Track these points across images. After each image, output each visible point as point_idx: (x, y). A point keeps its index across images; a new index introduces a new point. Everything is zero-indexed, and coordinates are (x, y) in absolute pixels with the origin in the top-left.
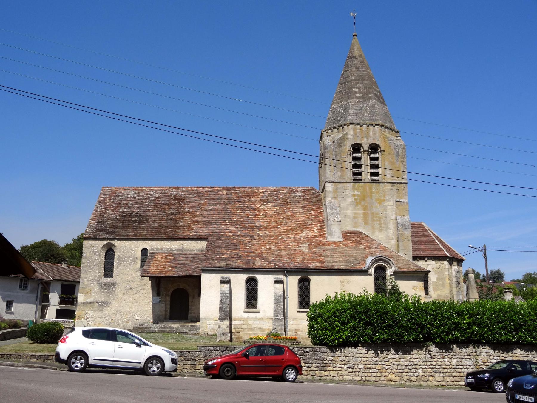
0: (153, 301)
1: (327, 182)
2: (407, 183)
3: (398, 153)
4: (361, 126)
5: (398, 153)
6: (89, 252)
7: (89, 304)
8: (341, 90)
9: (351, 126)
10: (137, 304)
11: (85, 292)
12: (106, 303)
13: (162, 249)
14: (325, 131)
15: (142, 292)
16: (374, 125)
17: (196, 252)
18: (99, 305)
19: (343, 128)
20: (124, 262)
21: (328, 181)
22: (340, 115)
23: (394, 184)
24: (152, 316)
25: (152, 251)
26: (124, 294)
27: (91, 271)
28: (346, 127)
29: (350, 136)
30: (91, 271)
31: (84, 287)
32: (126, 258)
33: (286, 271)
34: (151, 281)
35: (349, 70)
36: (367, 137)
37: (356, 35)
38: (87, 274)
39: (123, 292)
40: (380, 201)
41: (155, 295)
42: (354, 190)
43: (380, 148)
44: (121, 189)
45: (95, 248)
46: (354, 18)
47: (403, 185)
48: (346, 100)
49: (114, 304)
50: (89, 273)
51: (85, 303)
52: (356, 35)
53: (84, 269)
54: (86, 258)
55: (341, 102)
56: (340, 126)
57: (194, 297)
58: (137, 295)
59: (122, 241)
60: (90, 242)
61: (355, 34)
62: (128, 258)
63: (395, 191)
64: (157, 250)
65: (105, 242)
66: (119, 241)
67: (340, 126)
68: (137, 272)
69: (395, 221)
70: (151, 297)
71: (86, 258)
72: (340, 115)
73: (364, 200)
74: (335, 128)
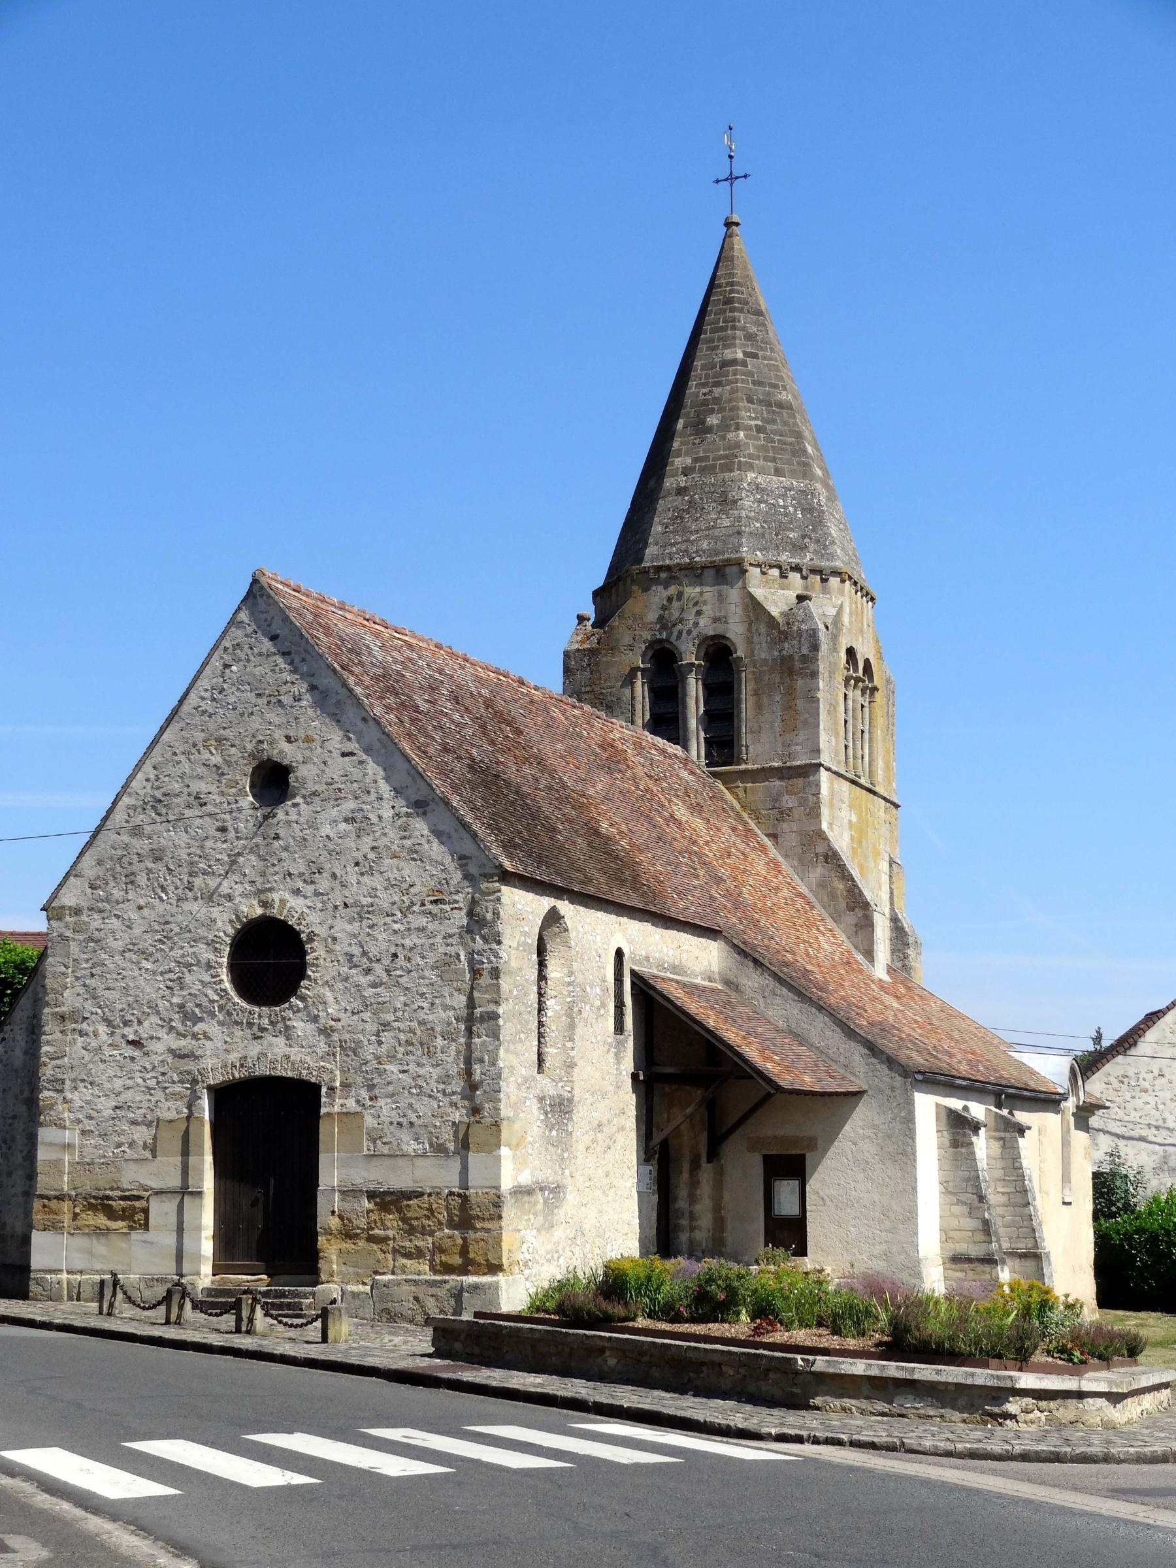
0: (639, 1181)
1: (822, 765)
2: (897, 806)
3: (888, 707)
4: (856, 592)
5: (888, 707)
6: (515, 945)
7: (526, 1198)
8: (760, 423)
9: (848, 582)
10: (611, 1193)
11: (514, 1142)
12: (557, 1190)
13: (647, 958)
14: (759, 565)
15: (620, 1138)
16: (869, 596)
17: (698, 981)
18: (546, 1201)
19: (824, 581)
20: (586, 1004)
21: (825, 764)
22: (791, 523)
23: (888, 804)
24: (637, 1244)
25: (634, 963)
26: (587, 1149)
27: (522, 1036)
28: (834, 581)
29: (846, 619)
30: (522, 1036)
31: (511, 1114)
32: (588, 989)
33: (1008, 1096)
34: (634, 1096)
35: (764, 358)
36: (861, 631)
37: (737, 224)
38: (516, 1054)
39: (586, 1140)
40: (877, 854)
41: (643, 1156)
42: (851, 807)
43: (871, 679)
44: (319, 603)
45: (526, 929)
46: (731, 157)
47: (894, 810)
48: (793, 474)
49: (571, 1197)
50: (519, 1046)
51: (523, 1192)
52: (737, 224)
53: (508, 1025)
54: (510, 973)
55: (778, 472)
56: (814, 571)
57: (695, 1165)
58: (611, 1156)
59: (578, 907)
60: (517, 898)
61: (736, 218)
62: (592, 986)
63: (888, 825)
64: (640, 963)
65: (546, 903)
66: (572, 907)
67: (814, 571)
68: (609, 1051)
69: (887, 923)
70: (635, 1162)
71: (510, 973)
72: (791, 523)
73: (860, 843)
74: (797, 568)
